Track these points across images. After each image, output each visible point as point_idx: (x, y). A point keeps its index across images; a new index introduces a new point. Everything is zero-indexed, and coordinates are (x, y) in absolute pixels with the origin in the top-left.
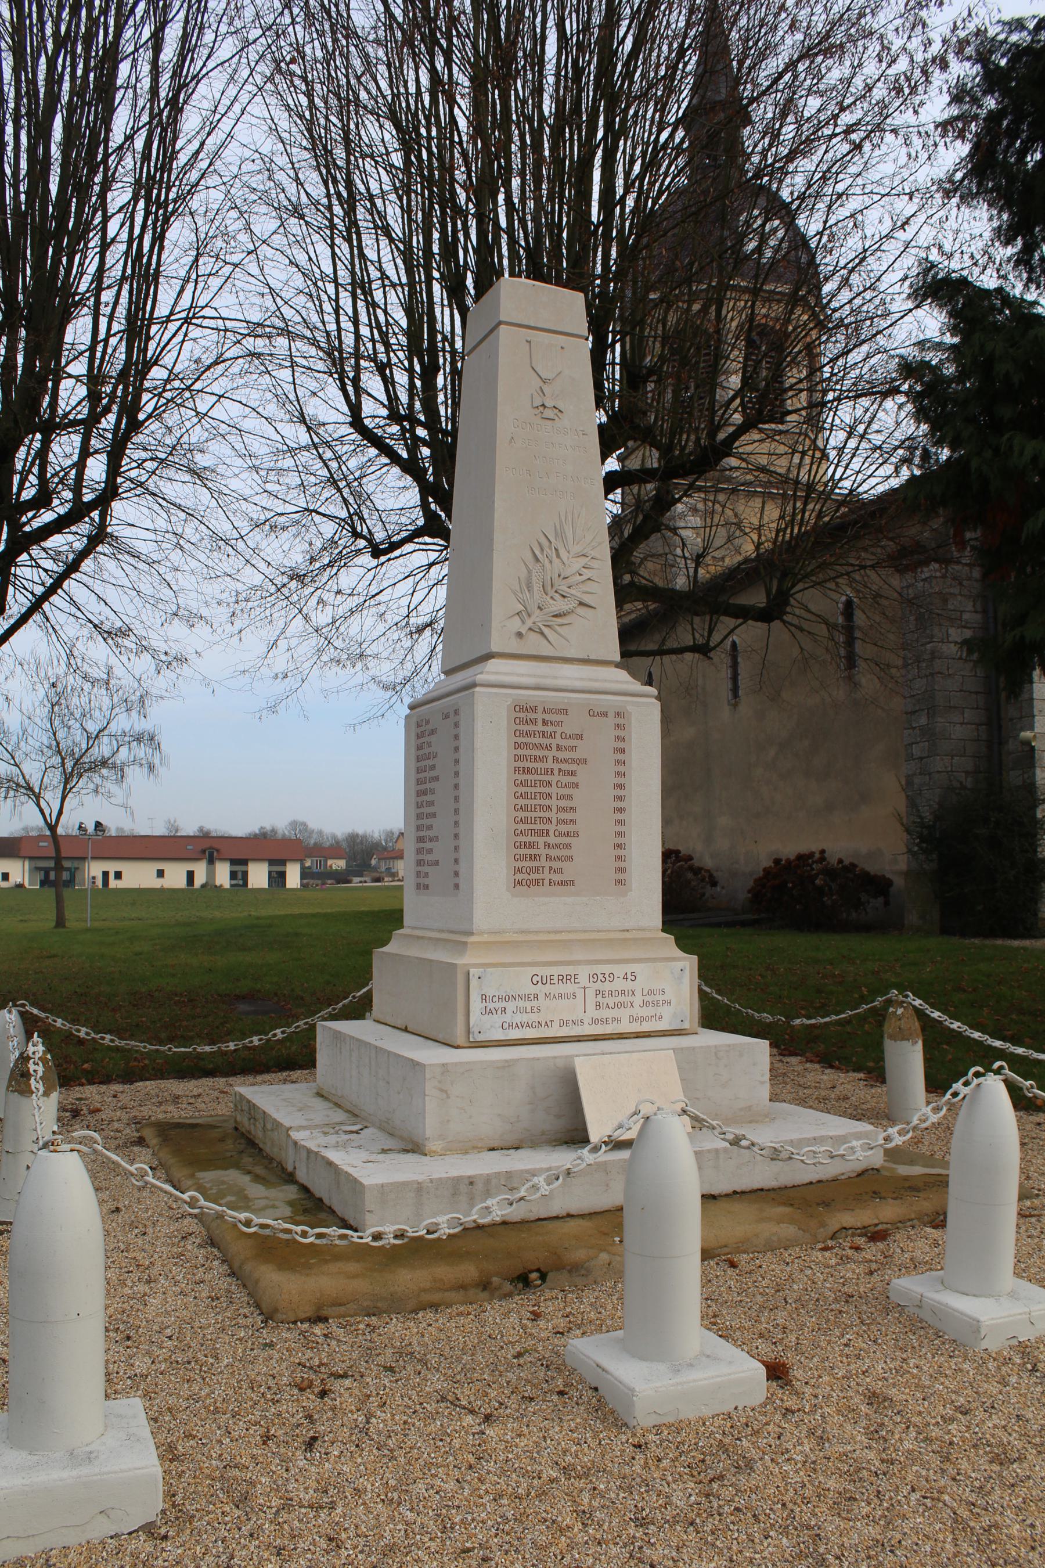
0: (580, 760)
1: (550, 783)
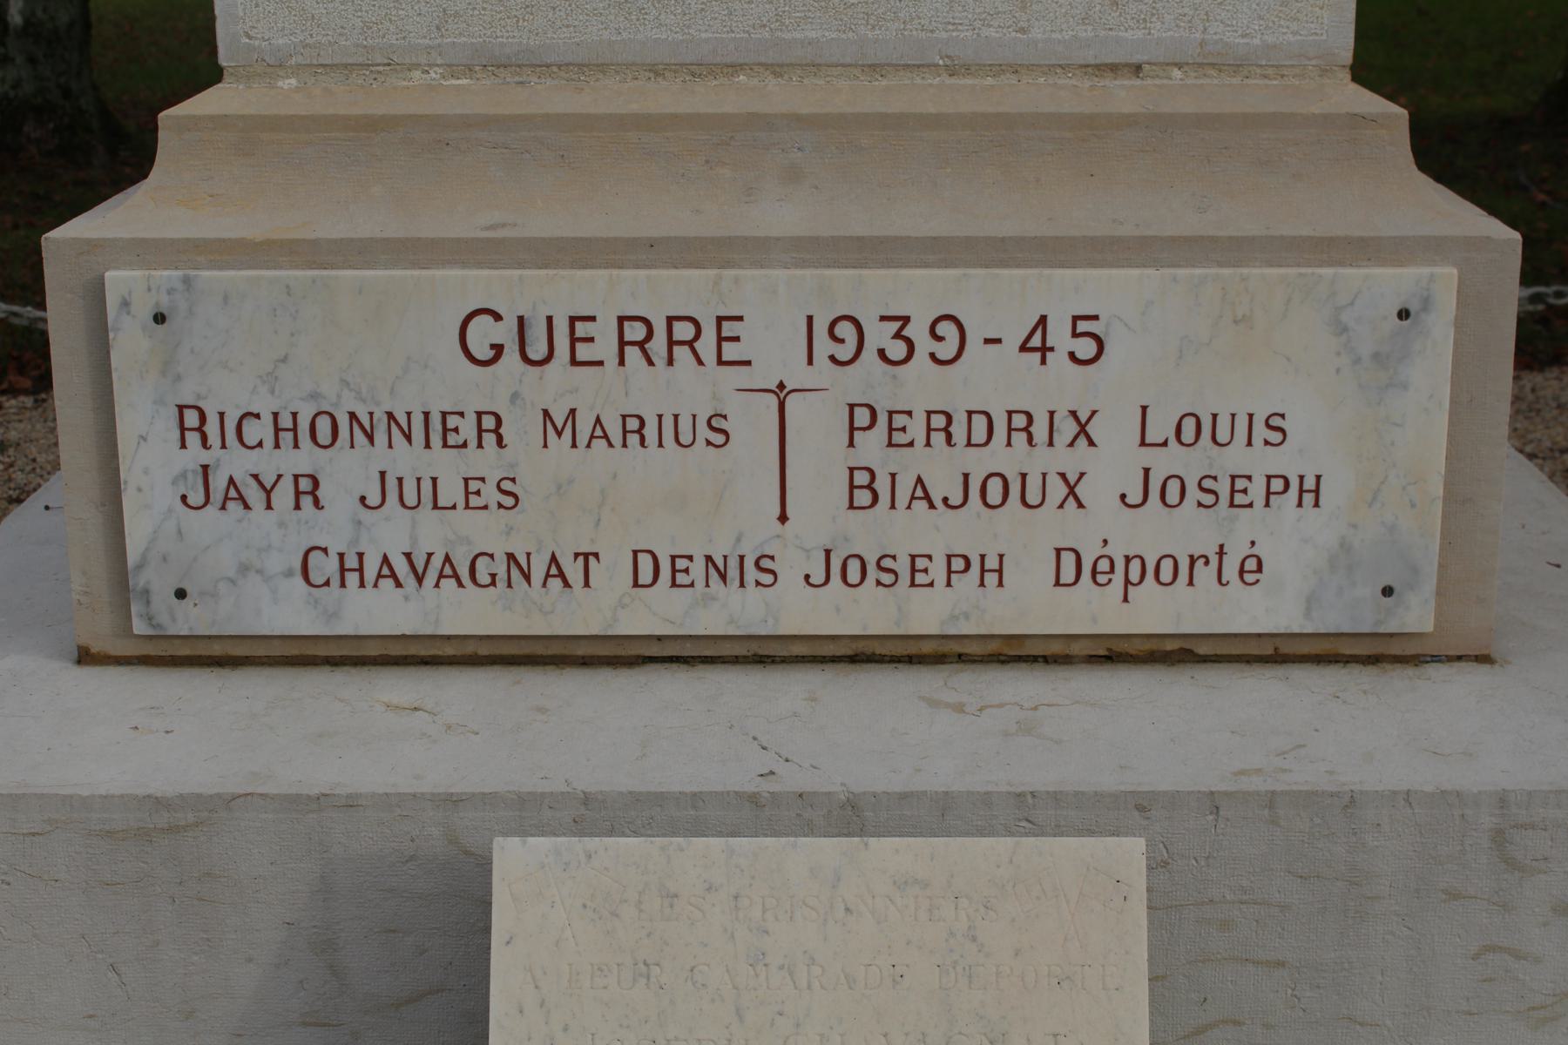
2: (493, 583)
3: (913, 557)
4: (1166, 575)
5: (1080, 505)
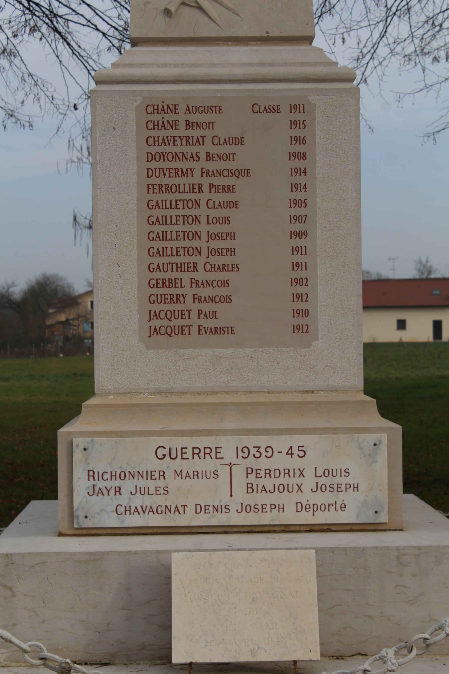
0: (240, 172)
1: (197, 204)
2: (162, 513)
3: (262, 505)
4: (323, 509)
5: (302, 492)
